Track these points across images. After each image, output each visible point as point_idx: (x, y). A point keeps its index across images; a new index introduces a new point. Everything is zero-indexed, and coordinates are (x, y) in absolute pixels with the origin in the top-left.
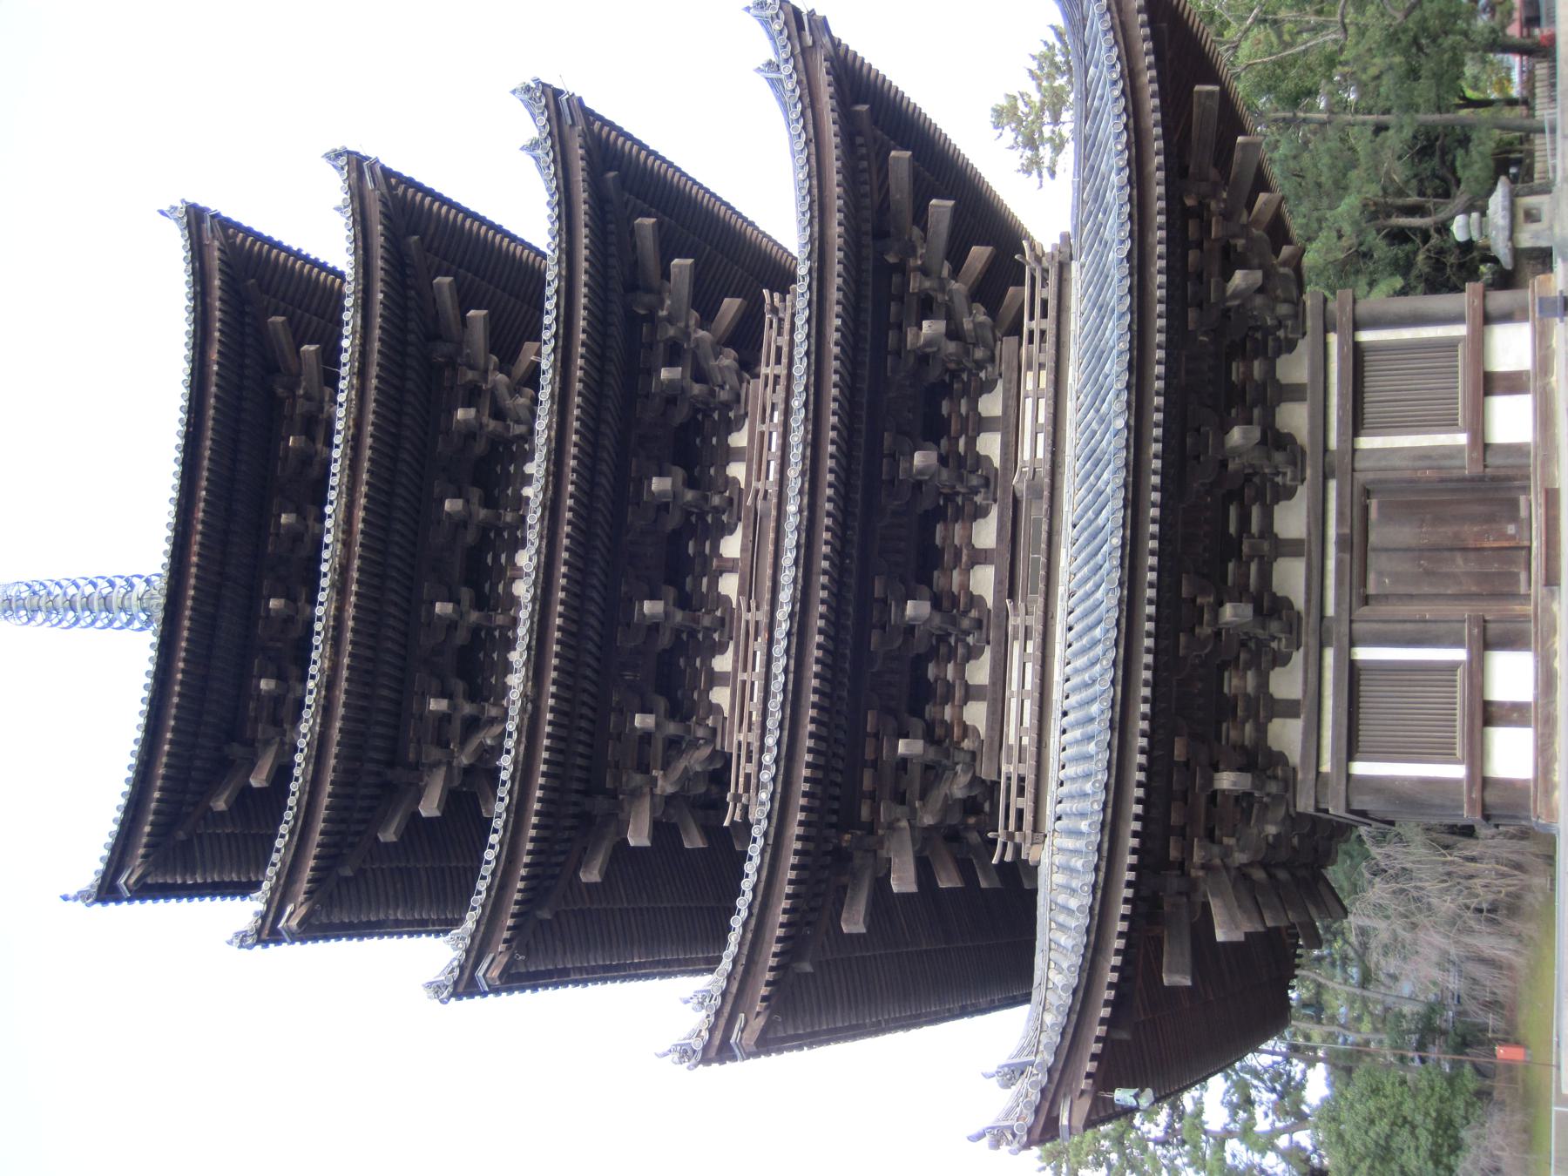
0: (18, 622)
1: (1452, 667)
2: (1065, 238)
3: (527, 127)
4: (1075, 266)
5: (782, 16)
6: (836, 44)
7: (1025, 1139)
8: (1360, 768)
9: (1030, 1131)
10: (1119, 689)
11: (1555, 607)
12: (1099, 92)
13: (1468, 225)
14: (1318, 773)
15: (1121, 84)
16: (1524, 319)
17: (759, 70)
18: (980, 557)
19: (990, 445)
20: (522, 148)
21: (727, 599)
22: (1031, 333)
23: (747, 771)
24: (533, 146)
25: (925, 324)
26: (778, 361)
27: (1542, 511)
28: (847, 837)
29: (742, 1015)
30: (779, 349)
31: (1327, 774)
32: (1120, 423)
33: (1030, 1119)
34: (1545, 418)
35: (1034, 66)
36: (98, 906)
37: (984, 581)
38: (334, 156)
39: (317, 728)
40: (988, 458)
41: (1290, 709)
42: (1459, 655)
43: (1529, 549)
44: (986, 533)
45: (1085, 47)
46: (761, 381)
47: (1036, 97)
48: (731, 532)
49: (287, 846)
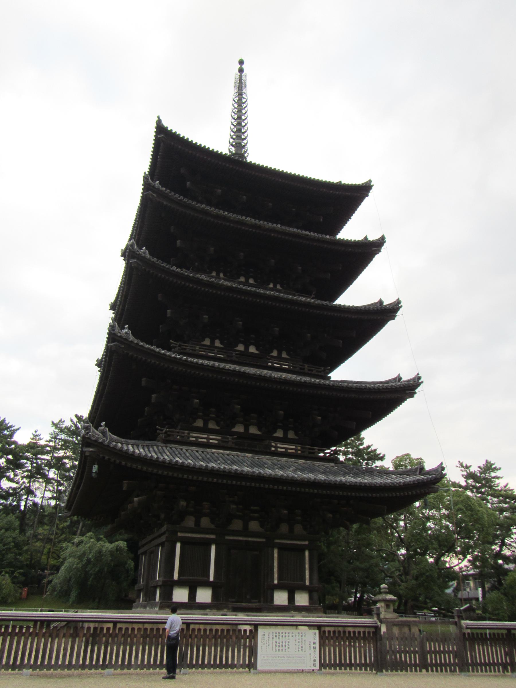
0: (234, 97)
1: (208, 576)
4: (333, 464)
5: (415, 384)
6: (406, 400)
7: (87, 437)
8: (178, 545)
9: (89, 438)
10: (222, 473)
11: (225, 610)
12: (389, 478)
13: (385, 588)
14: (177, 532)
15: (393, 485)
16: (310, 603)
17: (399, 375)
18: (247, 428)
19: (279, 434)
20: (380, 299)
21: (237, 346)
22: (314, 449)
23: (187, 350)
24: (381, 302)
25: (320, 418)
26: (309, 370)
27: (254, 607)
28: (170, 381)
29: (123, 346)
30: (312, 370)
31: (177, 535)
32: (298, 479)
33: (93, 439)
34: (281, 609)
35: (373, 448)
36: (155, 125)
37: (239, 429)
39: (212, 213)
40: (275, 432)
41: (197, 523)
42: (212, 579)
44: (253, 430)
45: (400, 475)
46: (301, 364)
47: (361, 447)
48: (257, 349)
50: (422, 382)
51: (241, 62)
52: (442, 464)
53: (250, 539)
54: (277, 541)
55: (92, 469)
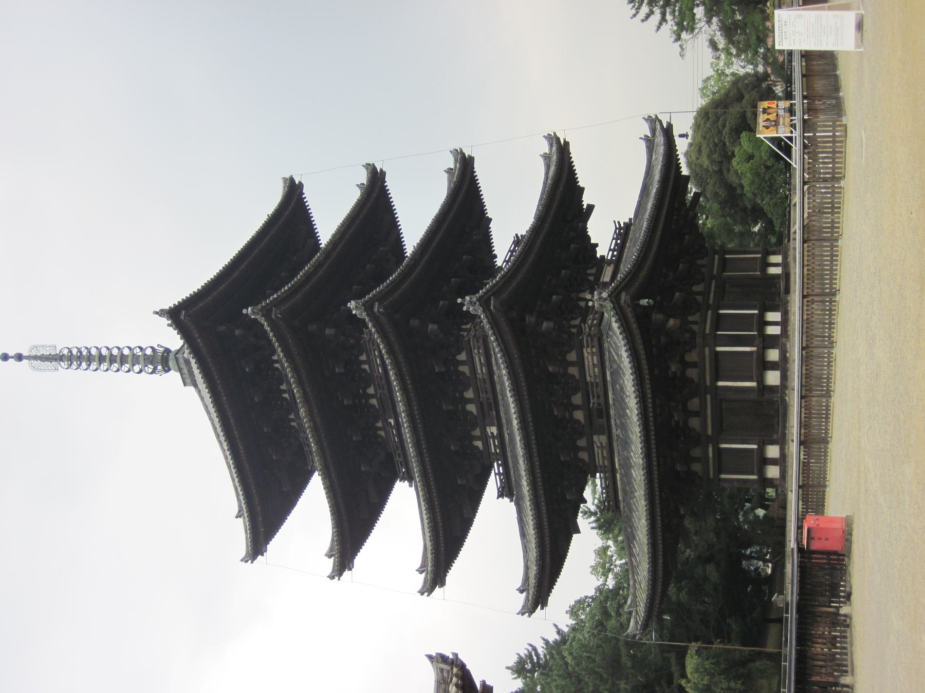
1: (754, 314)
2: (630, 219)
3: (450, 163)
4: (632, 227)
6: (570, 154)
9: (612, 293)
13: (770, 3)
16: (780, 254)
24: (449, 171)
27: (784, 282)
31: (707, 334)
38: (367, 166)
41: (696, 323)
42: (756, 312)
43: (780, 293)
49: (286, 291)
50: (555, 133)
51: (5, 357)
52: (644, 118)
53: (713, 289)
54: (715, 273)
55: (644, 307)
